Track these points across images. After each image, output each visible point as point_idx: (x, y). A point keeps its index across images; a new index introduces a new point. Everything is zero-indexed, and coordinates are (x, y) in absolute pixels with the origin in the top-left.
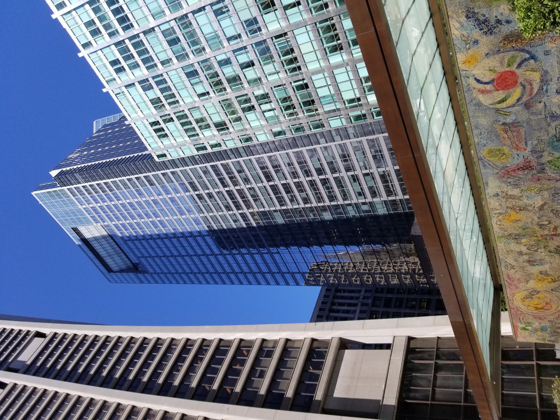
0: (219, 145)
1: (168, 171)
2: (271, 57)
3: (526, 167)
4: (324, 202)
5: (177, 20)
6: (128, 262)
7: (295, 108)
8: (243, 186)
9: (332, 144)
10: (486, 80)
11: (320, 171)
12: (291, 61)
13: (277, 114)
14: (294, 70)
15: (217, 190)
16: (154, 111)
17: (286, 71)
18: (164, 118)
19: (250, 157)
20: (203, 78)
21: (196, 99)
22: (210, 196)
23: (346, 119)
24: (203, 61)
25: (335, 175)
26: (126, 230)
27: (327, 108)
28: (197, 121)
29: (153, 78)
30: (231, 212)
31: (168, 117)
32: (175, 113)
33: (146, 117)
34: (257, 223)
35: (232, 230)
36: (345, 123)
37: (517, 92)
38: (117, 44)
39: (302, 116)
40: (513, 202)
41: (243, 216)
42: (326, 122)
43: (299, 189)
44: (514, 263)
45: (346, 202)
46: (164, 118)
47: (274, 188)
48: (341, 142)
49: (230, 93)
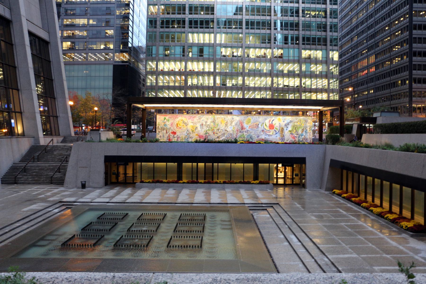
3: (242, 128)
10: (273, 122)
40: (229, 123)
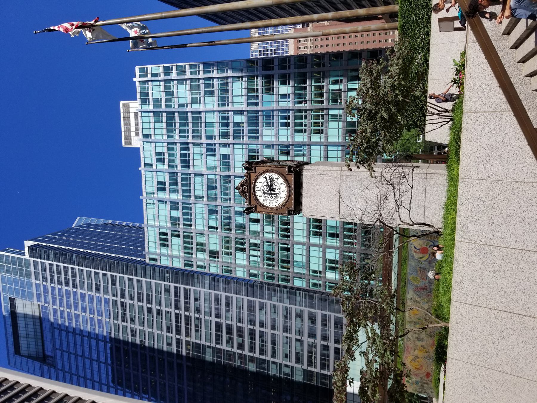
0: (204, 267)
1: (135, 278)
2: (273, 222)
3: (425, 289)
4: (254, 353)
5: (222, 176)
6: (41, 351)
7: (274, 261)
8: (192, 314)
9: (281, 305)
11: (262, 325)
12: (284, 230)
13: (259, 260)
14: (284, 236)
15: (168, 310)
16: (169, 225)
17: (279, 234)
18: (173, 232)
19: (211, 291)
20: (218, 217)
21: (206, 228)
22: (159, 312)
23: (307, 283)
24: (225, 207)
25: (273, 332)
26: (62, 317)
27: (296, 270)
28: (197, 244)
29: (183, 203)
30: (169, 334)
31: (177, 233)
32: (184, 232)
33: (159, 227)
34: (188, 354)
35: (160, 352)
36: (305, 286)
37: (427, 256)
38: (170, 173)
39: (277, 269)
41: (178, 342)
42: (292, 280)
43: (239, 333)
44: (411, 338)
45: (273, 360)
46: (173, 232)
47: (218, 326)
48: (288, 306)
49: (233, 234)
